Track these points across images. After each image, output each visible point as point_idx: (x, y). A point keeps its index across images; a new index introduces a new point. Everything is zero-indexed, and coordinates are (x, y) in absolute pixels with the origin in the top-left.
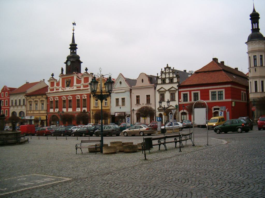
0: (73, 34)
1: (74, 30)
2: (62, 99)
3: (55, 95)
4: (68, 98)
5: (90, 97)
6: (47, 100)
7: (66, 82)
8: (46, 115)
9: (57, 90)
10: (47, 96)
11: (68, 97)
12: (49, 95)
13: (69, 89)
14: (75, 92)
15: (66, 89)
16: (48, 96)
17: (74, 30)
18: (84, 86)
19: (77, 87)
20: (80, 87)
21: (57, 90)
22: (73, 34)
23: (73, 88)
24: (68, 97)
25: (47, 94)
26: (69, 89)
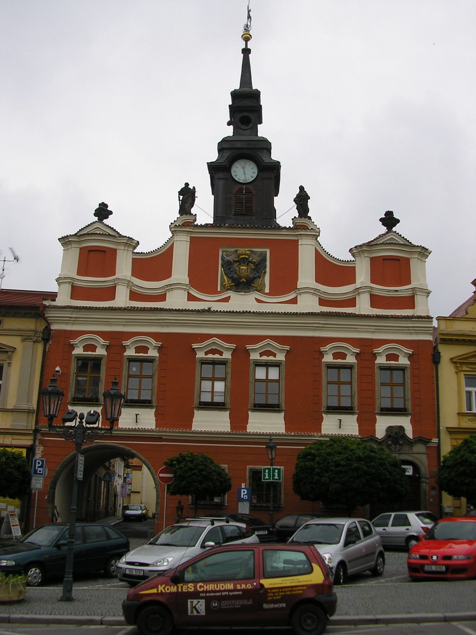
0: (246, 52)
1: (247, 39)
2: (194, 351)
3: (128, 322)
4: (247, 353)
5: (436, 359)
6: (40, 348)
7: (227, 265)
8: (28, 441)
9: (134, 296)
10: (49, 324)
11: (249, 347)
12: (76, 321)
13: (258, 301)
14: (322, 321)
15: (227, 300)
16: (54, 327)
17: (247, 39)
18: (376, 301)
19: (322, 302)
20: (352, 302)
21: (134, 296)
22: (246, 52)
23: (294, 301)
24: (249, 347)
25: (49, 314)
26: (258, 301)
